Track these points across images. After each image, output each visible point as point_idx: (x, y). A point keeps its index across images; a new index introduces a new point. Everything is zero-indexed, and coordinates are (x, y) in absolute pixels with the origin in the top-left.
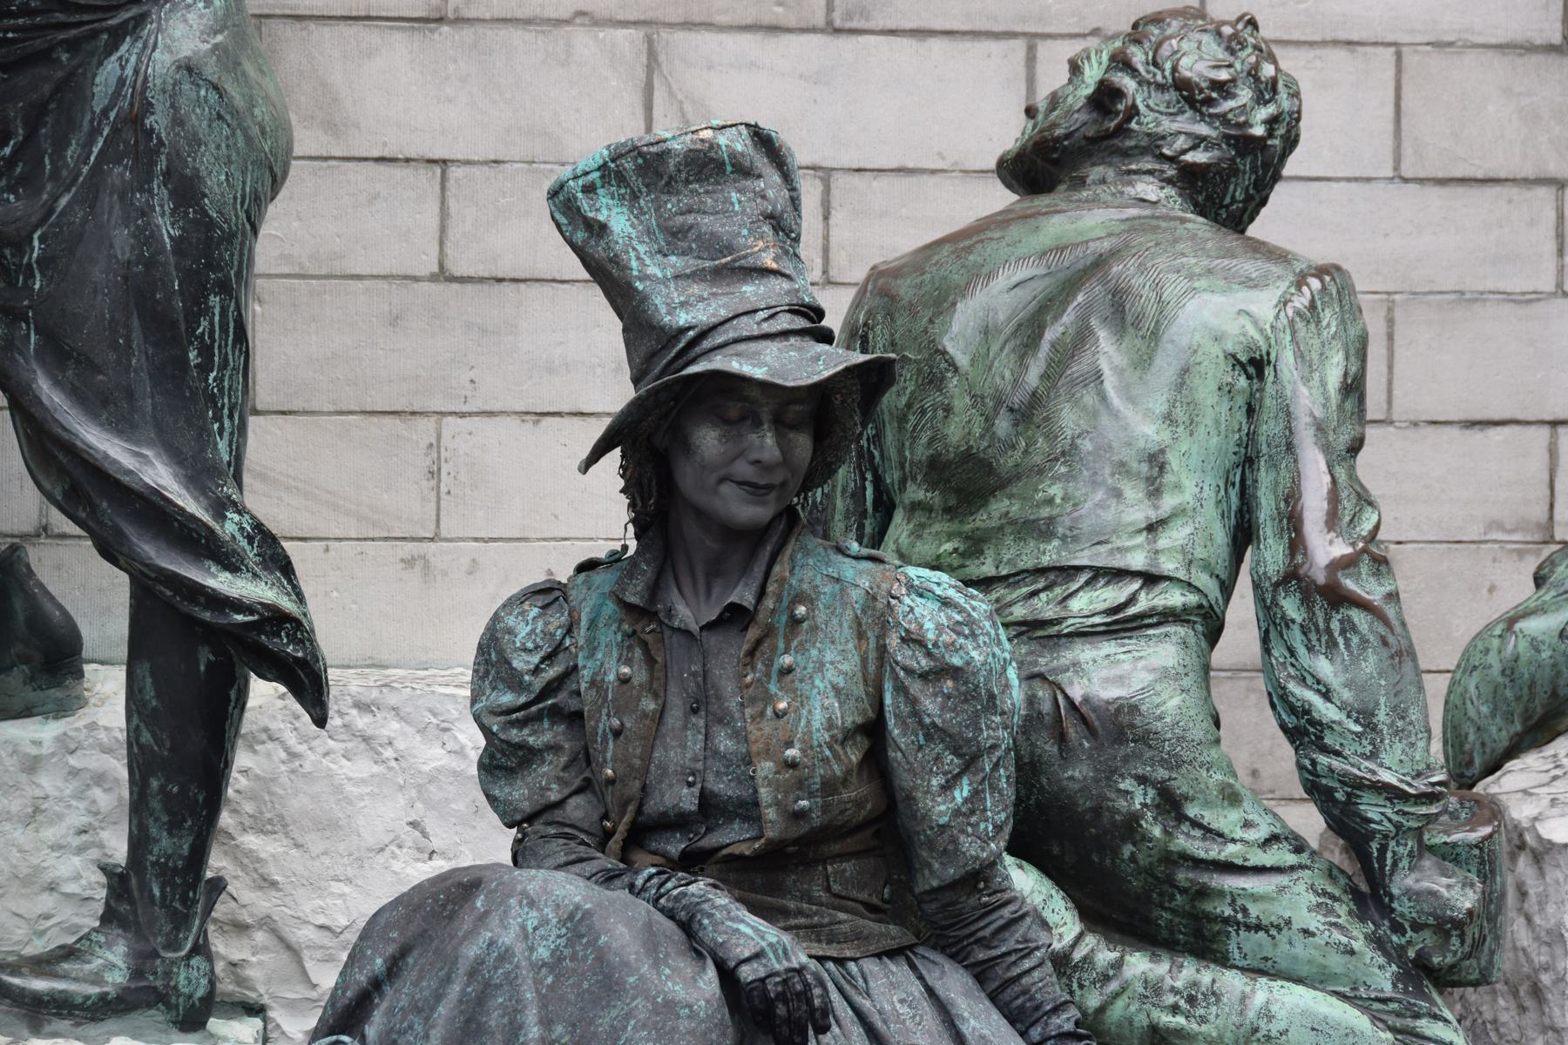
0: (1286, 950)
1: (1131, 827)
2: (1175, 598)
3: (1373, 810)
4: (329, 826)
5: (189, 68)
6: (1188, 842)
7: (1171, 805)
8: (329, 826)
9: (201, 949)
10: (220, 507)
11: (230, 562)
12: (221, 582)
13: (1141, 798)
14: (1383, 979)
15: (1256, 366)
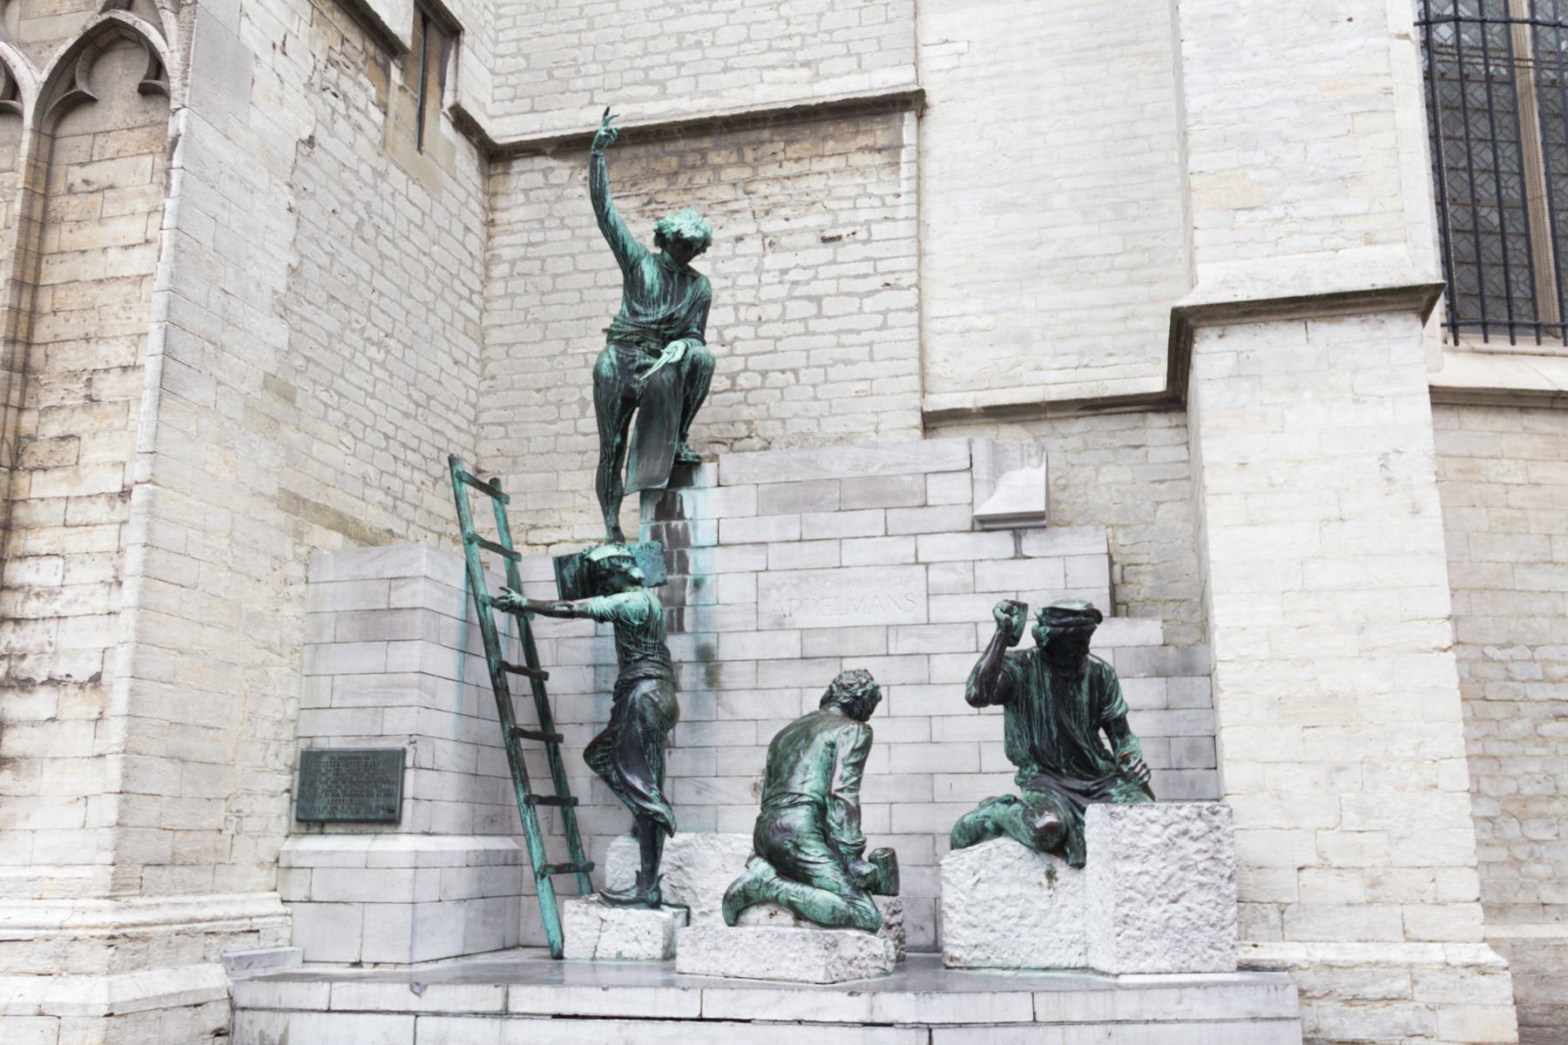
0: (825, 883)
1: (787, 852)
2: (806, 799)
3: (842, 849)
4: (704, 865)
5: (645, 695)
6: (802, 856)
7: (797, 847)
8: (704, 865)
9: (658, 890)
10: (651, 790)
11: (650, 800)
12: (648, 805)
13: (789, 846)
14: (847, 890)
15: (832, 745)
